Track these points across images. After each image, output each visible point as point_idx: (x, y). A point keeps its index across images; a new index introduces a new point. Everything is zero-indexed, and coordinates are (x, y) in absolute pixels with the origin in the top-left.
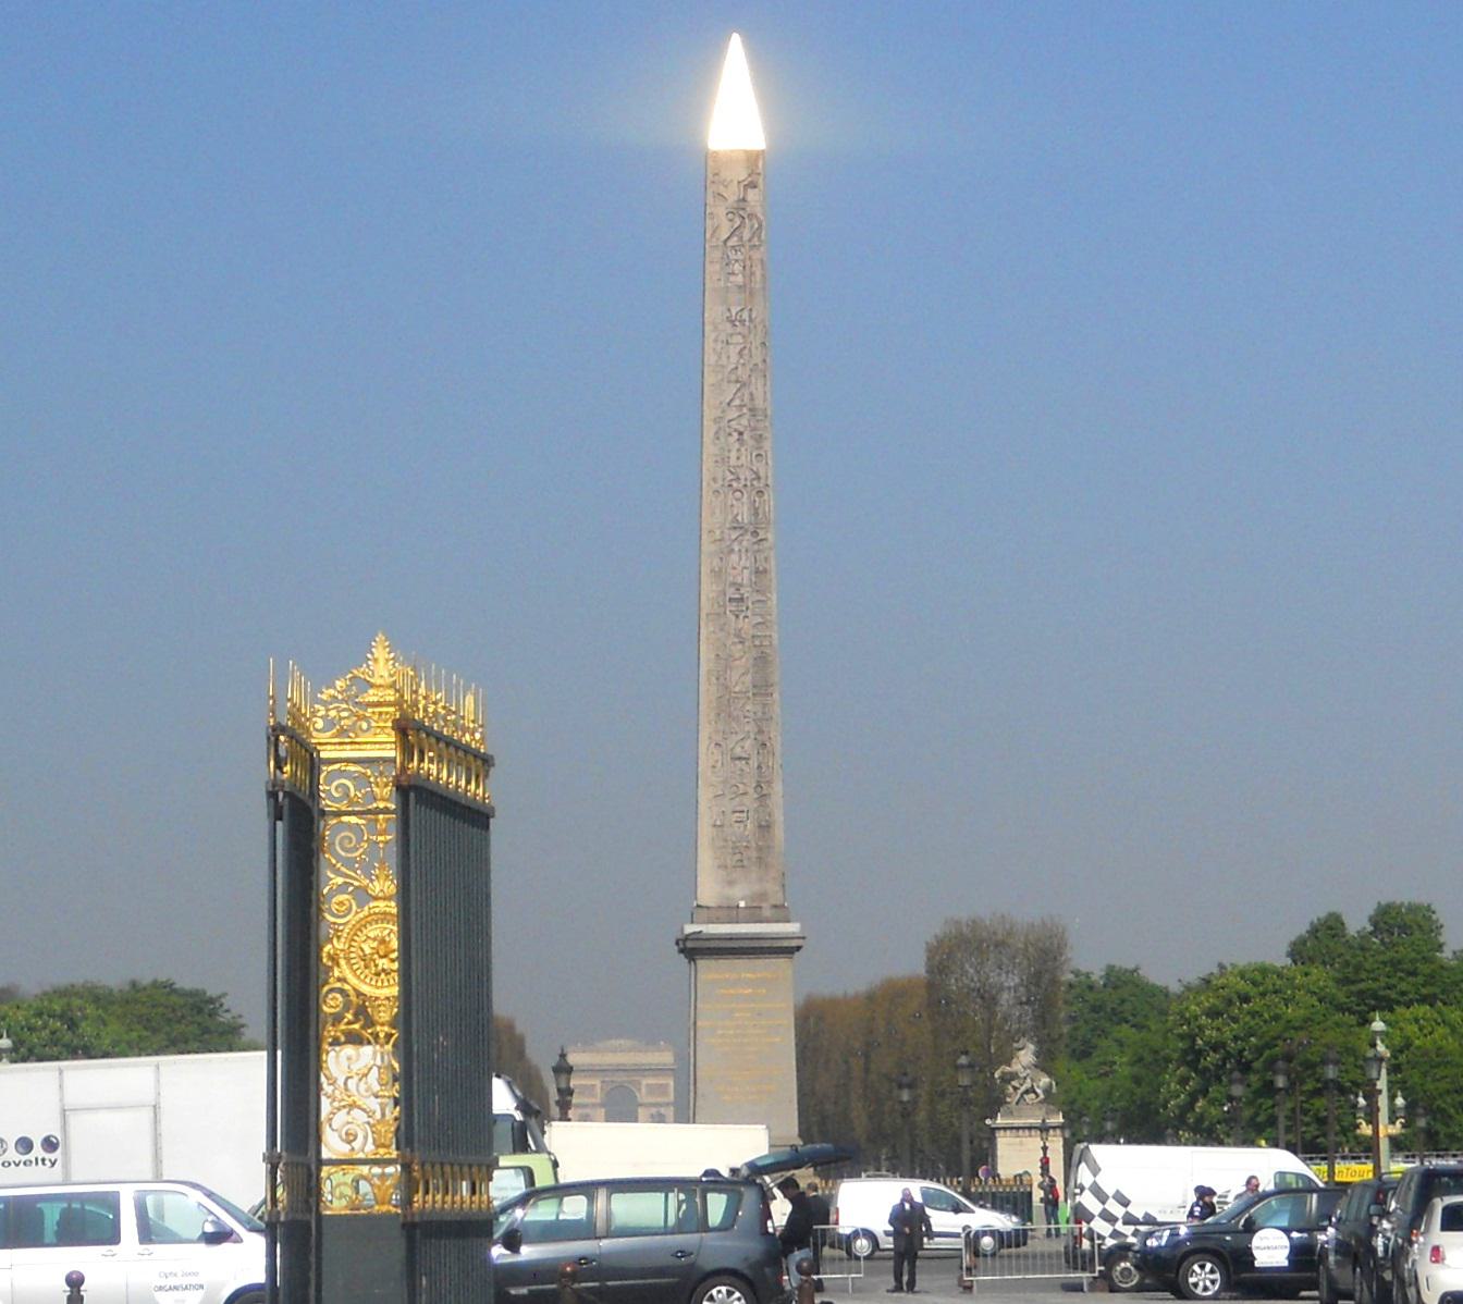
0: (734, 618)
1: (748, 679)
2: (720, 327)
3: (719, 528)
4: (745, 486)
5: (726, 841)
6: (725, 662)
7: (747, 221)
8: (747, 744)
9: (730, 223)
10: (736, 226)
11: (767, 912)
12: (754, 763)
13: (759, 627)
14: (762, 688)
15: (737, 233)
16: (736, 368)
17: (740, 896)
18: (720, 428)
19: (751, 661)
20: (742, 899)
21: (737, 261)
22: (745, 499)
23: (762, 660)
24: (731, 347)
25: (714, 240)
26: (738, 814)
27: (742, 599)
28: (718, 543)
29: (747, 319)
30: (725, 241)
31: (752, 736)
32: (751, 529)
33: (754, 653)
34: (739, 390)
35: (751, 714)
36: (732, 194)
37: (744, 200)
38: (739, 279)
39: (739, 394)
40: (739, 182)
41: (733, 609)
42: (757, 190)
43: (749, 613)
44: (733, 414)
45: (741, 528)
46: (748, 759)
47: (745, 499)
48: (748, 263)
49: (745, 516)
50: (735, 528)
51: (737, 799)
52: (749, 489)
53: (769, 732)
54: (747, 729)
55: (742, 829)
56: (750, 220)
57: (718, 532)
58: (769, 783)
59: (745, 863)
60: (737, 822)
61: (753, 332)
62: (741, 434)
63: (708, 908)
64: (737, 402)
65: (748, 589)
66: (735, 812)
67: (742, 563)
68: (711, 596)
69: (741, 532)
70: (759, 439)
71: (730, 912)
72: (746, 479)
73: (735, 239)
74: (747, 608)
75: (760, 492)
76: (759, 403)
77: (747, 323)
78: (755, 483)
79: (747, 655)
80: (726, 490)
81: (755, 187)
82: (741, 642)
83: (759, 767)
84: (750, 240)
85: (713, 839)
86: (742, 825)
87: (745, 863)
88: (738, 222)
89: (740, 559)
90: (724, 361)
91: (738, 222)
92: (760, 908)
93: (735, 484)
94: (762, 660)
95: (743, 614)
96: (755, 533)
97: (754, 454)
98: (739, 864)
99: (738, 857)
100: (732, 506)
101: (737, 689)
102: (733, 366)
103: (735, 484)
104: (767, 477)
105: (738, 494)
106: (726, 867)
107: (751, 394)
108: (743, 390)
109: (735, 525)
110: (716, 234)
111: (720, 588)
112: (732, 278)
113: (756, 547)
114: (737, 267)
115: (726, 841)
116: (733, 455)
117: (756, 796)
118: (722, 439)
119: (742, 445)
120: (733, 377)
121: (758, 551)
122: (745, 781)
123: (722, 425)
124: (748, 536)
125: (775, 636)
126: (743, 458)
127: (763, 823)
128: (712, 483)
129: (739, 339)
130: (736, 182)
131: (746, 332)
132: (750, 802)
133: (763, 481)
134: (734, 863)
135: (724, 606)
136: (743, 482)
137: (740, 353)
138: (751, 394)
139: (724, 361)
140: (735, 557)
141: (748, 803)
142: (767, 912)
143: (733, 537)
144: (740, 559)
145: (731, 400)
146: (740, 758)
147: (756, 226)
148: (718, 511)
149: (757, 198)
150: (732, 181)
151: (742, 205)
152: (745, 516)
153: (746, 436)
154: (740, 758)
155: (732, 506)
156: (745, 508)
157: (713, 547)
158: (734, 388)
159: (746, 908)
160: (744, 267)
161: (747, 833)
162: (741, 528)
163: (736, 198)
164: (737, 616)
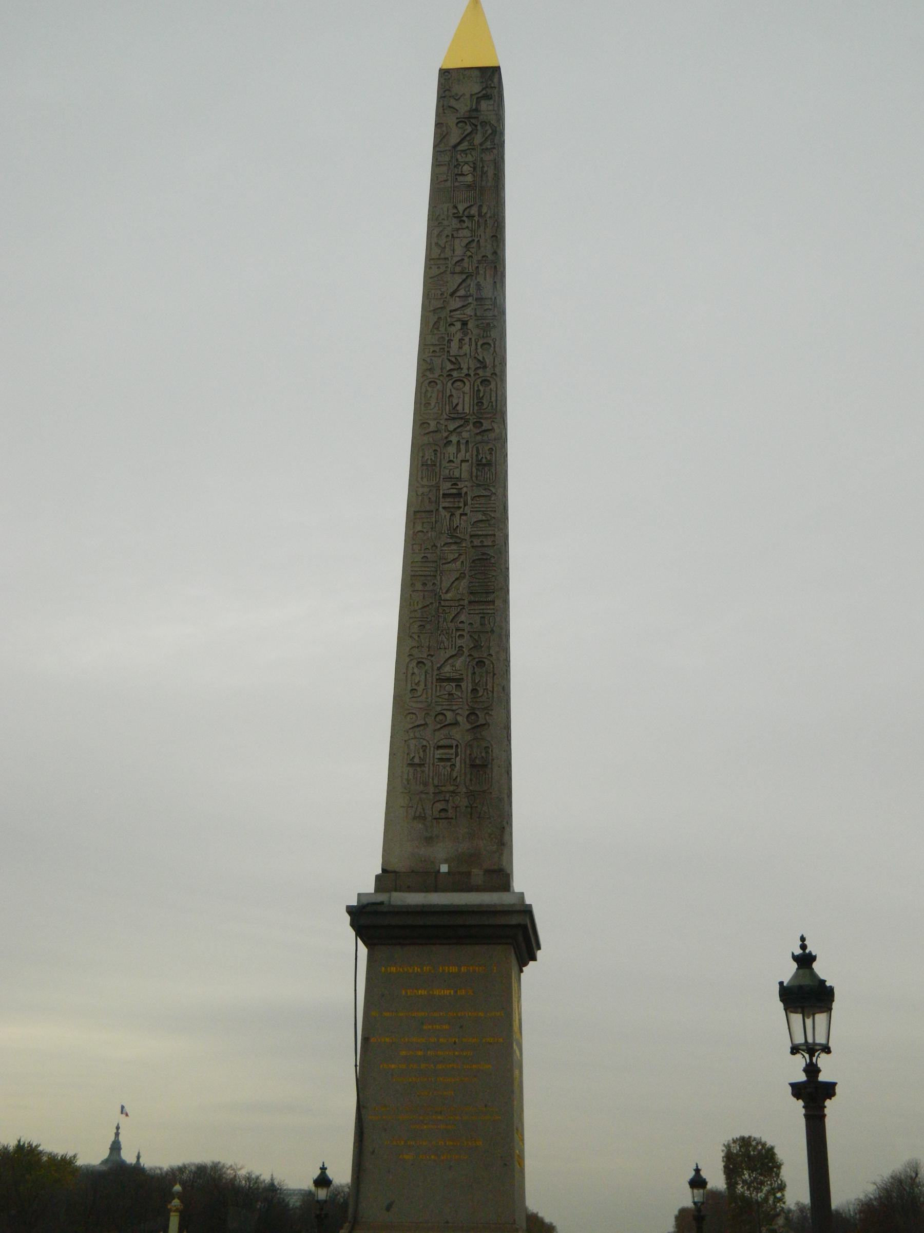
1: (464, 583)
2: (446, 223)
3: (435, 419)
4: (468, 375)
5: (426, 784)
7: (479, 127)
8: (459, 663)
10: (466, 133)
12: (467, 685)
15: (468, 138)
16: (463, 260)
18: (440, 318)
20: (446, 861)
21: (466, 163)
22: (467, 389)
24: (457, 241)
25: (442, 145)
26: (441, 751)
27: (459, 495)
28: (431, 434)
29: (477, 214)
31: (466, 652)
32: (473, 419)
34: (464, 281)
35: (465, 626)
37: (476, 110)
38: (469, 178)
39: (464, 285)
40: (472, 95)
41: (447, 505)
42: (491, 102)
43: (467, 510)
44: (456, 304)
45: (462, 418)
46: (461, 680)
48: (479, 164)
49: (466, 405)
50: (454, 419)
51: (442, 731)
52: (472, 378)
53: (489, 648)
54: (459, 642)
57: (433, 424)
59: (451, 813)
60: (441, 760)
61: (482, 228)
62: (464, 323)
63: (395, 872)
64: (461, 292)
66: (439, 747)
67: (461, 456)
69: (462, 422)
72: (469, 369)
73: (466, 143)
75: (486, 382)
77: (476, 219)
78: (480, 372)
79: (463, 557)
82: (455, 543)
83: (474, 690)
84: (481, 144)
85: (408, 780)
87: (451, 813)
89: (459, 451)
90: (448, 253)
91: (469, 129)
92: (469, 873)
93: (455, 374)
95: (461, 511)
97: (479, 344)
98: (443, 815)
99: (440, 806)
100: (451, 396)
101: (449, 596)
103: (455, 374)
105: (459, 383)
106: (424, 818)
108: (468, 281)
109: (456, 416)
112: (461, 179)
113: (479, 438)
114: (466, 169)
116: (455, 345)
117: (469, 726)
118: (442, 329)
119: (465, 334)
120: (458, 269)
122: (454, 708)
123: (443, 315)
126: (466, 348)
127: (478, 762)
128: (428, 373)
130: (468, 96)
132: (458, 735)
134: (436, 814)
135: (437, 503)
136: (465, 371)
139: (448, 253)
140: (452, 449)
144: (459, 451)
146: (449, 680)
147: (490, 131)
150: (464, 94)
151: (474, 114)
153: (471, 325)
154: (449, 680)
155: (451, 396)
158: (458, 279)
159: (449, 873)
160: (475, 169)
161: (455, 774)
162: (462, 418)
163: (468, 108)
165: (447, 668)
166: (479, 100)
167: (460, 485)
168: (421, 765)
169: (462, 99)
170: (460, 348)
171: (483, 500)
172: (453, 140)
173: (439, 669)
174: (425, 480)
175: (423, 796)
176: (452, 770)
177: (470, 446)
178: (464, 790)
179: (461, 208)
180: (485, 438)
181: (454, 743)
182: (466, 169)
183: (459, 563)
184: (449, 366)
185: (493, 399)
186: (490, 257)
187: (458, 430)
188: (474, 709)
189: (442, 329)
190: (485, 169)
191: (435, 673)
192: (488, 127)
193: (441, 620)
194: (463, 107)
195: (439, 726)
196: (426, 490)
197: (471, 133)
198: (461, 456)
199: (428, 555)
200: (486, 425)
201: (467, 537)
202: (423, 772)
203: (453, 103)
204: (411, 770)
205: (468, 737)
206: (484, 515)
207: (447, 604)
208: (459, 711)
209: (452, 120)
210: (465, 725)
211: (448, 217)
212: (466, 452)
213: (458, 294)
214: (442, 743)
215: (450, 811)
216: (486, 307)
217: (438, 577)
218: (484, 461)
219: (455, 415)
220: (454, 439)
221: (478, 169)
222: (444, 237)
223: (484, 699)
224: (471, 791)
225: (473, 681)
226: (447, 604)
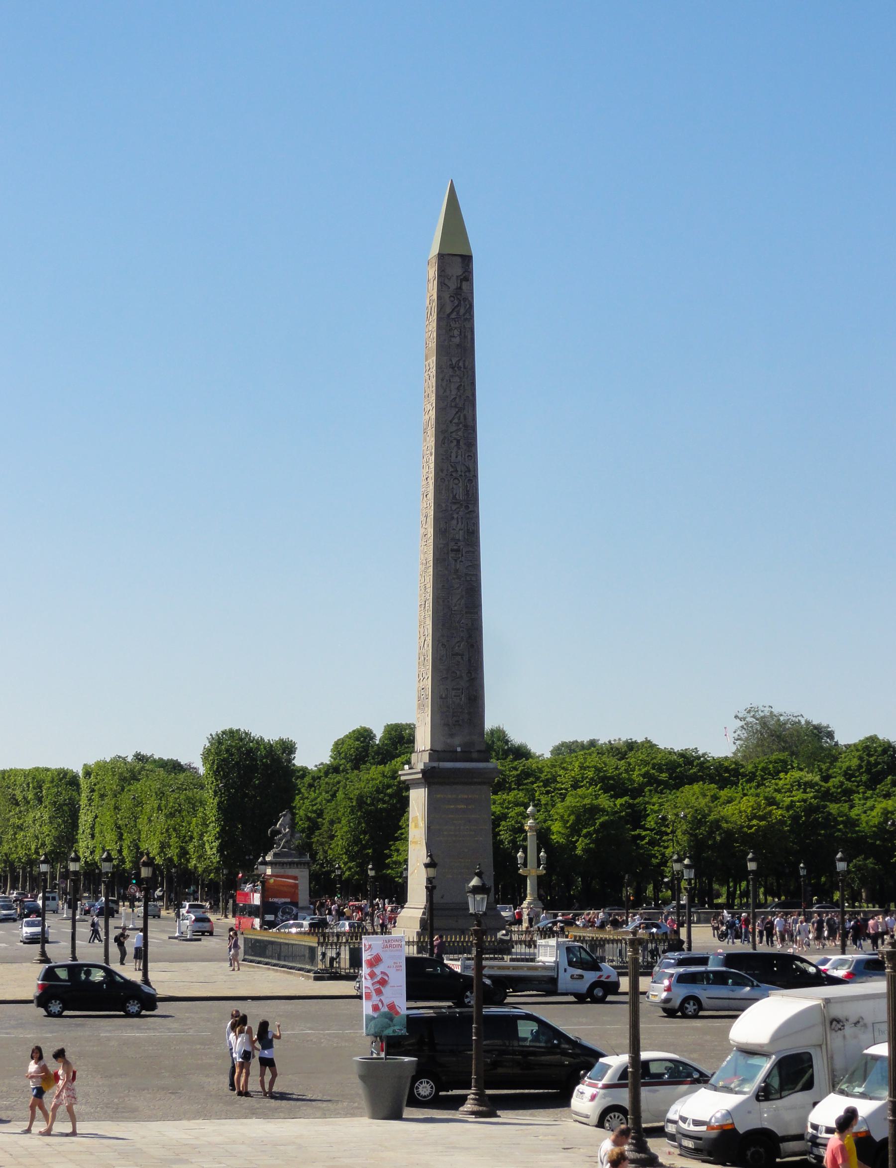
1: (463, 601)
5: (448, 707)
27: (458, 550)
30: (449, 315)
37: (460, 288)
38: (457, 340)
46: (462, 655)
47: (460, 484)
49: (461, 496)
56: (465, 301)
57: (444, 505)
62: (458, 441)
64: (456, 421)
83: (469, 660)
84: (464, 315)
91: (456, 302)
93: (454, 474)
96: (467, 507)
102: (453, 397)
103: (454, 474)
105: (456, 481)
107: (465, 416)
112: (453, 339)
113: (468, 516)
114: (456, 333)
116: (454, 455)
119: (459, 448)
120: (453, 404)
126: (459, 457)
129: (457, 379)
130: (455, 277)
133: (472, 473)
135: (448, 553)
137: (458, 389)
138: (465, 416)
140: (454, 522)
145: (453, 419)
146: (457, 654)
152: (461, 496)
154: (457, 654)
158: (454, 411)
164: (456, 561)
166: (461, 281)
168: (446, 697)
172: (448, 310)
184: (451, 469)
186: (471, 398)
194: (453, 285)
197: (457, 306)
203: (446, 281)
209: (446, 296)
219: (455, 501)
220: (455, 516)
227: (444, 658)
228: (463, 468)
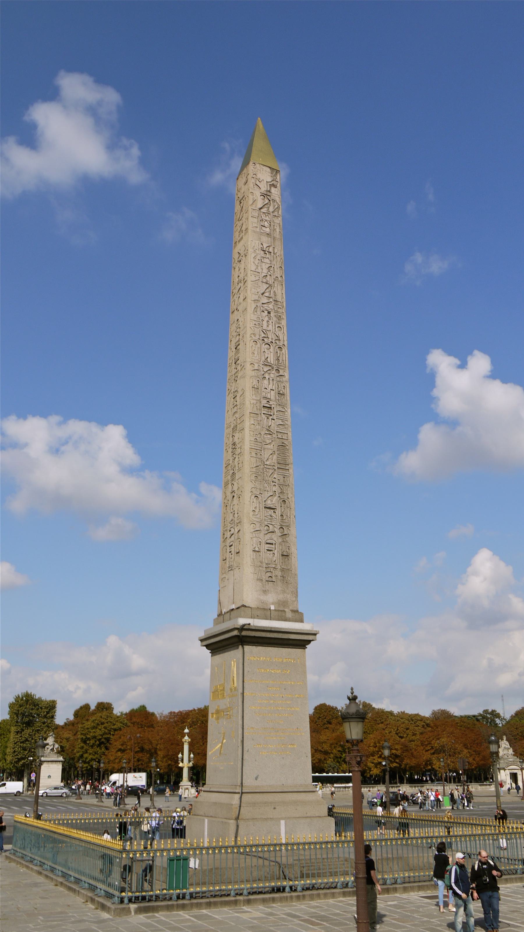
0: (266, 418)
1: (275, 457)
2: (257, 251)
3: (258, 363)
5: (261, 562)
6: (259, 448)
7: (271, 202)
8: (275, 499)
9: (262, 201)
11: (289, 615)
13: (281, 427)
14: (283, 465)
15: (266, 206)
17: (271, 599)
19: (276, 449)
20: (273, 604)
23: (282, 447)
24: (263, 264)
29: (272, 252)
30: (260, 209)
31: (277, 495)
33: (278, 442)
35: (276, 480)
36: (264, 188)
37: (269, 191)
38: (268, 230)
39: (267, 290)
42: (277, 189)
47: (271, 350)
48: (272, 224)
49: (272, 359)
50: (266, 365)
52: (274, 345)
53: (288, 494)
54: (274, 489)
55: (272, 555)
58: (288, 526)
62: (269, 313)
65: (275, 403)
66: (267, 543)
68: (252, 402)
69: (270, 368)
70: (279, 318)
71: (265, 612)
72: (272, 339)
73: (266, 209)
74: (274, 414)
76: (279, 298)
77: (272, 254)
78: (277, 342)
79: (273, 443)
80: (261, 342)
81: (276, 187)
83: (282, 515)
84: (273, 212)
85: (253, 559)
86: (272, 552)
87: (274, 579)
88: (267, 201)
89: (269, 384)
92: (284, 611)
93: (266, 340)
94: (282, 447)
96: (278, 371)
97: (277, 326)
98: (270, 579)
99: (269, 574)
101: (268, 463)
103: (266, 340)
104: (284, 341)
106: (262, 580)
107: (274, 292)
108: (270, 288)
110: (254, 203)
111: (258, 399)
112: (263, 228)
113: (278, 379)
115: (261, 562)
116: (265, 323)
117: (280, 535)
120: (264, 281)
121: (280, 381)
122: (273, 523)
124: (274, 372)
125: (290, 434)
126: (270, 326)
128: (253, 336)
130: (265, 182)
131: (272, 259)
132: (276, 538)
135: (260, 410)
138: (274, 292)
139: (259, 270)
140: (266, 382)
141: (275, 539)
142: (289, 615)
143: (265, 371)
147: (276, 206)
148: (256, 353)
149: (276, 193)
152: (272, 359)
153: (272, 314)
156: (272, 354)
157: (254, 373)
158: (265, 286)
159: (275, 610)
160: (270, 225)
161: (275, 559)
165: (269, 502)
167: (271, 403)
169: (262, 182)
170: (268, 326)
171: (281, 413)
173: (265, 501)
174: (254, 396)
175: (261, 568)
176: (273, 556)
177: (275, 382)
178: (280, 568)
179: (265, 246)
180: (281, 379)
181: (274, 542)
182: (266, 224)
183: (272, 445)
184: (263, 335)
185: (284, 359)
187: (269, 372)
188: (282, 525)
189: (259, 313)
190: (275, 227)
191: (264, 503)
192: (275, 204)
193: (265, 475)
195: (267, 532)
196: (255, 402)
198: (271, 387)
199: (258, 439)
200: (281, 373)
201: (275, 432)
202: (260, 555)
203: (258, 183)
204: (255, 554)
205: (280, 540)
206: (282, 422)
207: (267, 467)
208: (275, 526)
210: (278, 533)
211: (259, 249)
212: (273, 385)
213: (265, 295)
214: (268, 542)
215: (274, 578)
216: (279, 306)
217: (263, 451)
218: (281, 392)
220: (267, 376)
221: (272, 226)
222: (257, 260)
223: (286, 521)
224: (283, 569)
225: (281, 511)
226: (267, 467)
227: (257, 510)
228: (274, 337)
